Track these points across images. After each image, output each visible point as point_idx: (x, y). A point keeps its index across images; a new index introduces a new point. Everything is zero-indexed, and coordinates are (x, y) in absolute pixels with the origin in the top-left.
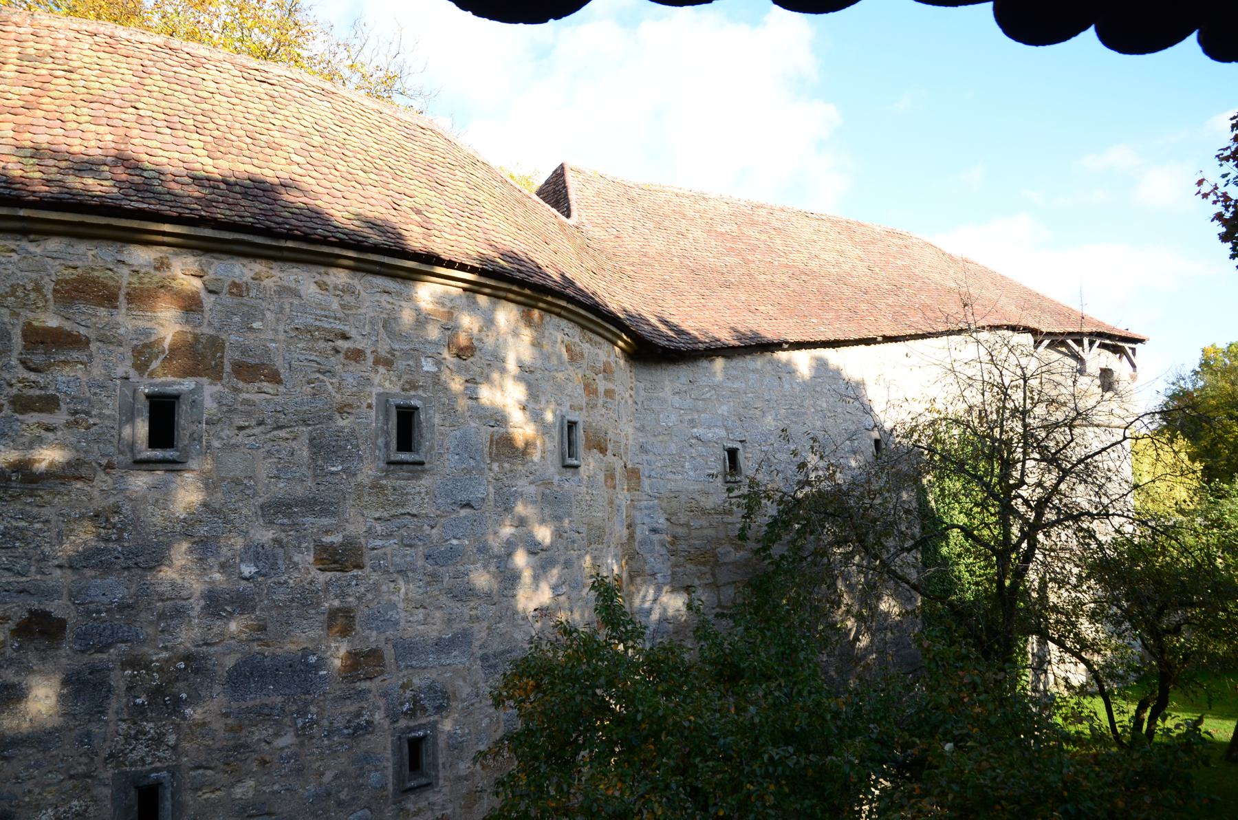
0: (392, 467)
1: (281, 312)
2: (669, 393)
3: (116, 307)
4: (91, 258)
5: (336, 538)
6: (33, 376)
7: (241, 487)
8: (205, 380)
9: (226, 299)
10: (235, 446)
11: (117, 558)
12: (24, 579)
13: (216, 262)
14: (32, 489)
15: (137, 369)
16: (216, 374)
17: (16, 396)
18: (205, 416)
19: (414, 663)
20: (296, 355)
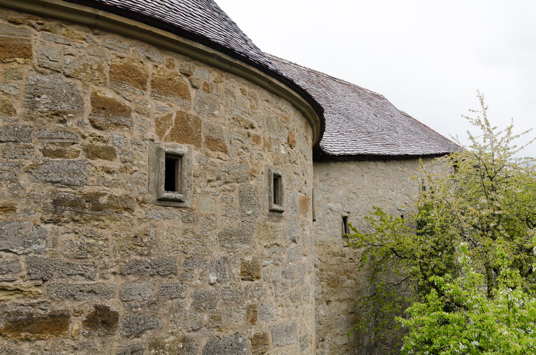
0: (271, 213)
1: (227, 106)
2: (318, 181)
3: (145, 89)
4: (132, 52)
5: (249, 259)
6: (98, 133)
7: (210, 221)
8: (192, 146)
9: (201, 92)
10: (208, 193)
11: (147, 268)
12: (92, 282)
13: (197, 68)
14: (98, 215)
15: (158, 135)
16: (196, 142)
17: (89, 145)
18: (193, 171)
19: (279, 343)
20: (233, 136)
